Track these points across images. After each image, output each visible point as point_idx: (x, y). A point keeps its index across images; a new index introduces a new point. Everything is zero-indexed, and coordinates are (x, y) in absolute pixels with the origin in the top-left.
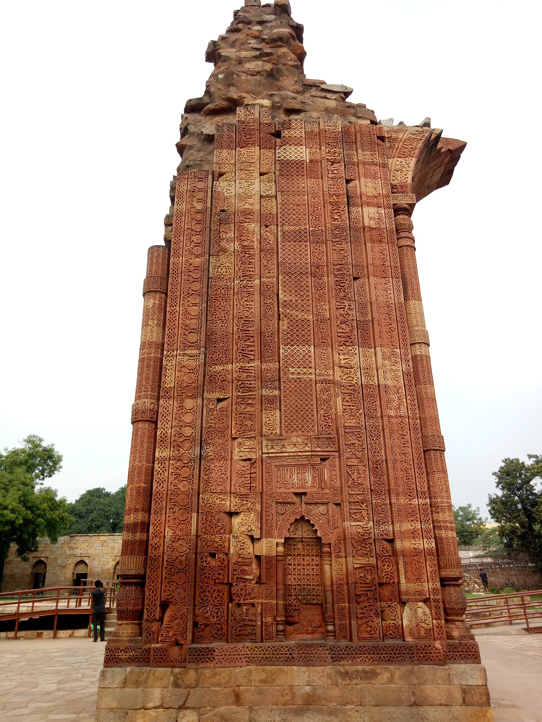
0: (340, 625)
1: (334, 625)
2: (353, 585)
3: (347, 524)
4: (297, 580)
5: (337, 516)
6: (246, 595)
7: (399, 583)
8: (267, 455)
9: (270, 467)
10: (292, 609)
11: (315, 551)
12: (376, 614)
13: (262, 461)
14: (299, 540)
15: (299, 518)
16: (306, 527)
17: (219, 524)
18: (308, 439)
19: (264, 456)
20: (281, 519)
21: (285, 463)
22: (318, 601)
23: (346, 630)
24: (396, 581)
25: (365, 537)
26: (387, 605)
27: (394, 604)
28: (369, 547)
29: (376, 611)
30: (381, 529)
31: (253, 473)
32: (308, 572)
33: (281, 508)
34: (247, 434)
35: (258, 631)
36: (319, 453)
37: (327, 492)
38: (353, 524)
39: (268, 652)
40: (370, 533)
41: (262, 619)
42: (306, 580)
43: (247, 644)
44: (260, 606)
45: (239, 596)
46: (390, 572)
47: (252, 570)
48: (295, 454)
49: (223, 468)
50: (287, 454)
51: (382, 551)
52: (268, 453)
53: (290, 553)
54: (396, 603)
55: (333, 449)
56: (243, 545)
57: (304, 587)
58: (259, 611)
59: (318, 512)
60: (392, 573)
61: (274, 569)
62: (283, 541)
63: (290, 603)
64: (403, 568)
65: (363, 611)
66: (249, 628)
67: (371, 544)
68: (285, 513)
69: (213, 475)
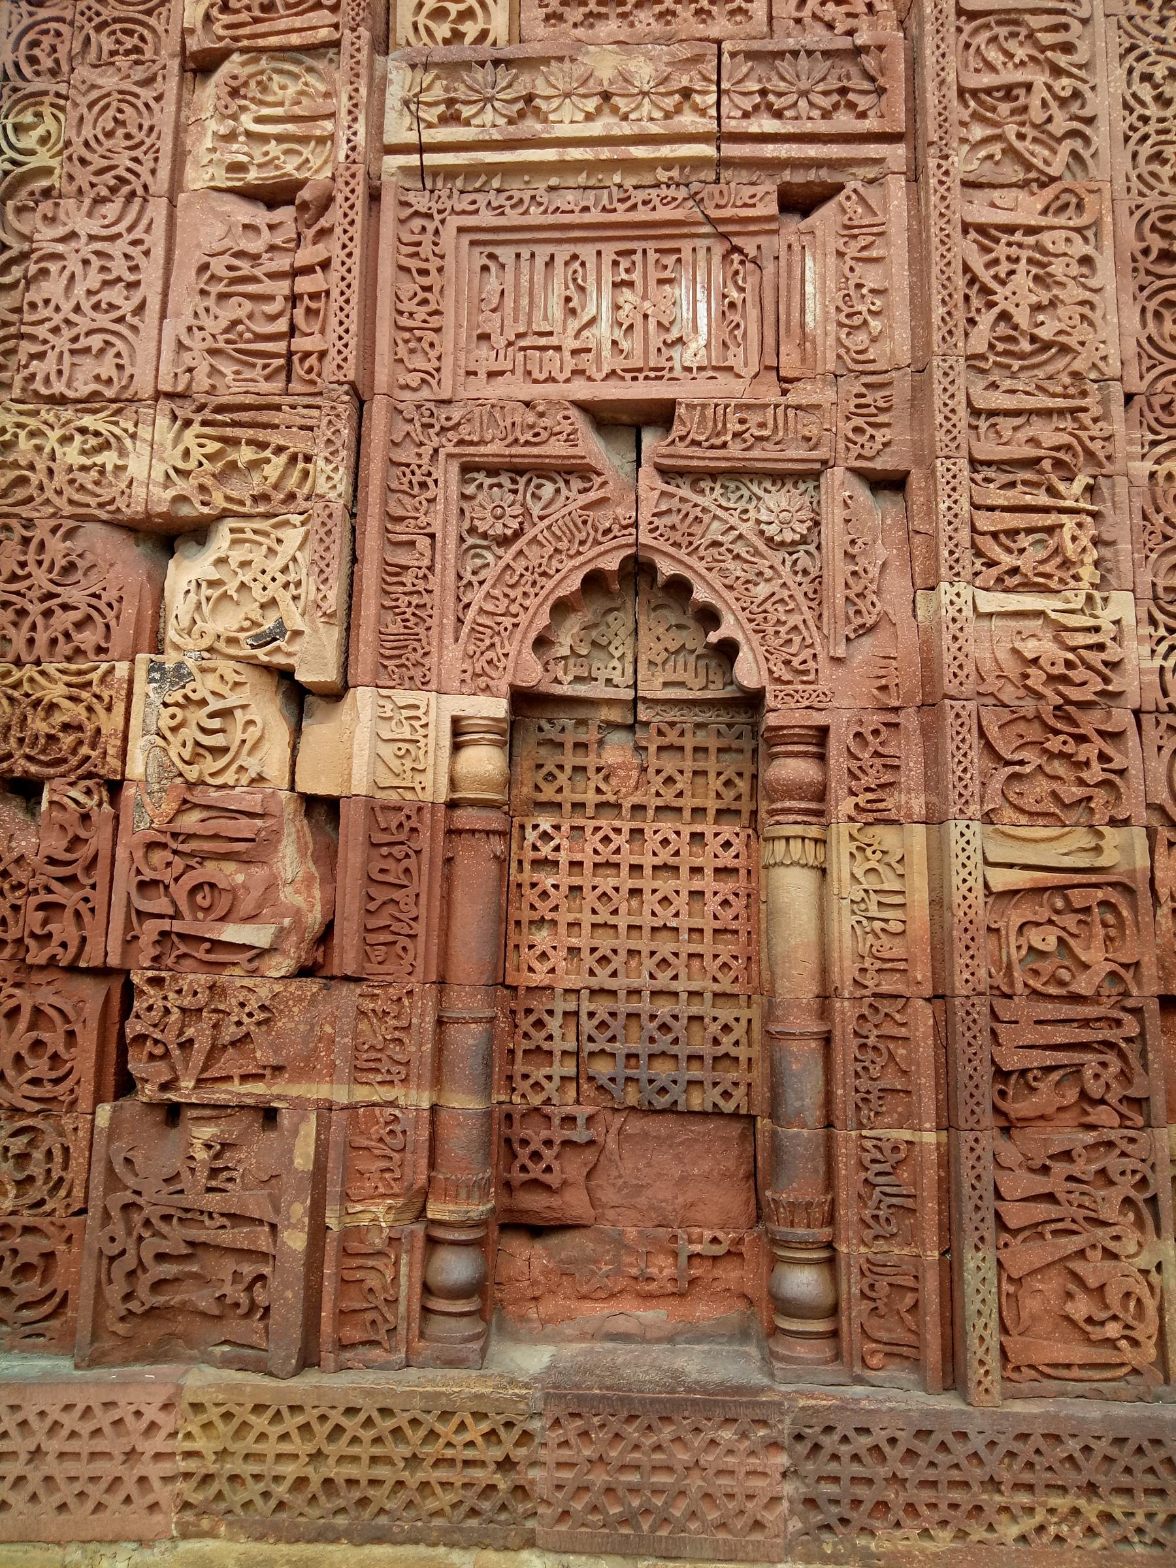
0: (872, 1268)
1: (831, 1263)
3: (955, 596)
4: (589, 960)
6: (214, 1052)
8: (413, 160)
9: (427, 239)
10: (548, 1143)
11: (716, 784)
13: (374, 196)
14: (615, 715)
15: (611, 564)
16: (660, 633)
17: (70, 594)
18: (698, 59)
19: (393, 162)
20: (489, 574)
21: (535, 216)
22: (726, 1095)
25: (1075, 694)
28: (1103, 757)
29: (1143, 1183)
31: (308, 270)
32: (665, 916)
33: (494, 504)
34: (282, 24)
35: (286, 1296)
36: (769, 151)
37: (814, 399)
38: (991, 602)
39: (341, 1446)
41: (317, 1211)
42: (649, 964)
43: (202, 1379)
44: (309, 1128)
45: (166, 1055)
47: (271, 886)
48: (605, 153)
49: (117, 249)
50: (550, 155)
52: (422, 149)
53: (548, 793)
55: (870, 124)
56: (216, 723)
57: (633, 1006)
58: (303, 1158)
59: (744, 528)
61: (426, 881)
62: (499, 707)
63: (536, 1100)
65: (1042, 1185)
66: (229, 1265)
67: (1115, 737)
68: (518, 534)
69: (52, 288)
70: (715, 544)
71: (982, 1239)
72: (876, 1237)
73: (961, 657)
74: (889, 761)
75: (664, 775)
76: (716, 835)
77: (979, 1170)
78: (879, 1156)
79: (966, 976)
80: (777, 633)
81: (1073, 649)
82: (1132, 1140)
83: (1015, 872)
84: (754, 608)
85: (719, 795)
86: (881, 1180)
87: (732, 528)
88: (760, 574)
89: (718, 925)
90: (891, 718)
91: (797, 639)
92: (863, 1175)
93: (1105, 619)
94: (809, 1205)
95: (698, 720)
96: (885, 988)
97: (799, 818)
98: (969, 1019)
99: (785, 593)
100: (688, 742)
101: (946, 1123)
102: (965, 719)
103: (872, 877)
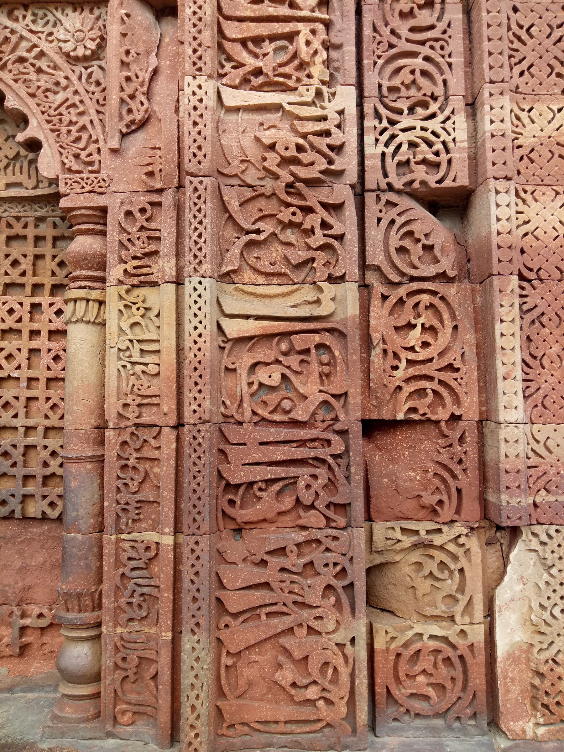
2: (207, 434)
5: (153, 62)
7: (486, 420)
12: (341, 592)
23: (155, 677)
24: (470, 408)
25: (303, 172)
26: (407, 541)
27: (448, 533)
28: (325, 225)
30: (403, 137)
40: (338, 149)
46: (437, 364)
51: (401, 250)
54: (459, 529)
60: (450, 368)
64: (516, 342)
65: (260, 575)
67: (336, 208)
70: (22, 60)
71: (198, 624)
72: (131, 620)
73: (200, 140)
74: (152, 234)
75: (11, 258)
76: (51, 305)
77: (198, 568)
78: (134, 555)
79: (194, 407)
80: (69, 132)
81: (304, 136)
82: (335, 538)
83: (251, 321)
84: (52, 112)
85: (53, 274)
86: (136, 573)
87: (35, 46)
88: (57, 84)
89: (50, 375)
90: (155, 198)
91: (85, 136)
92: (121, 571)
93: (330, 109)
94: (79, 595)
95: (38, 214)
96: (145, 419)
97: (84, 284)
98: (195, 443)
99: (77, 99)
100: (31, 232)
101: (177, 531)
102: (201, 191)
103: (137, 329)
